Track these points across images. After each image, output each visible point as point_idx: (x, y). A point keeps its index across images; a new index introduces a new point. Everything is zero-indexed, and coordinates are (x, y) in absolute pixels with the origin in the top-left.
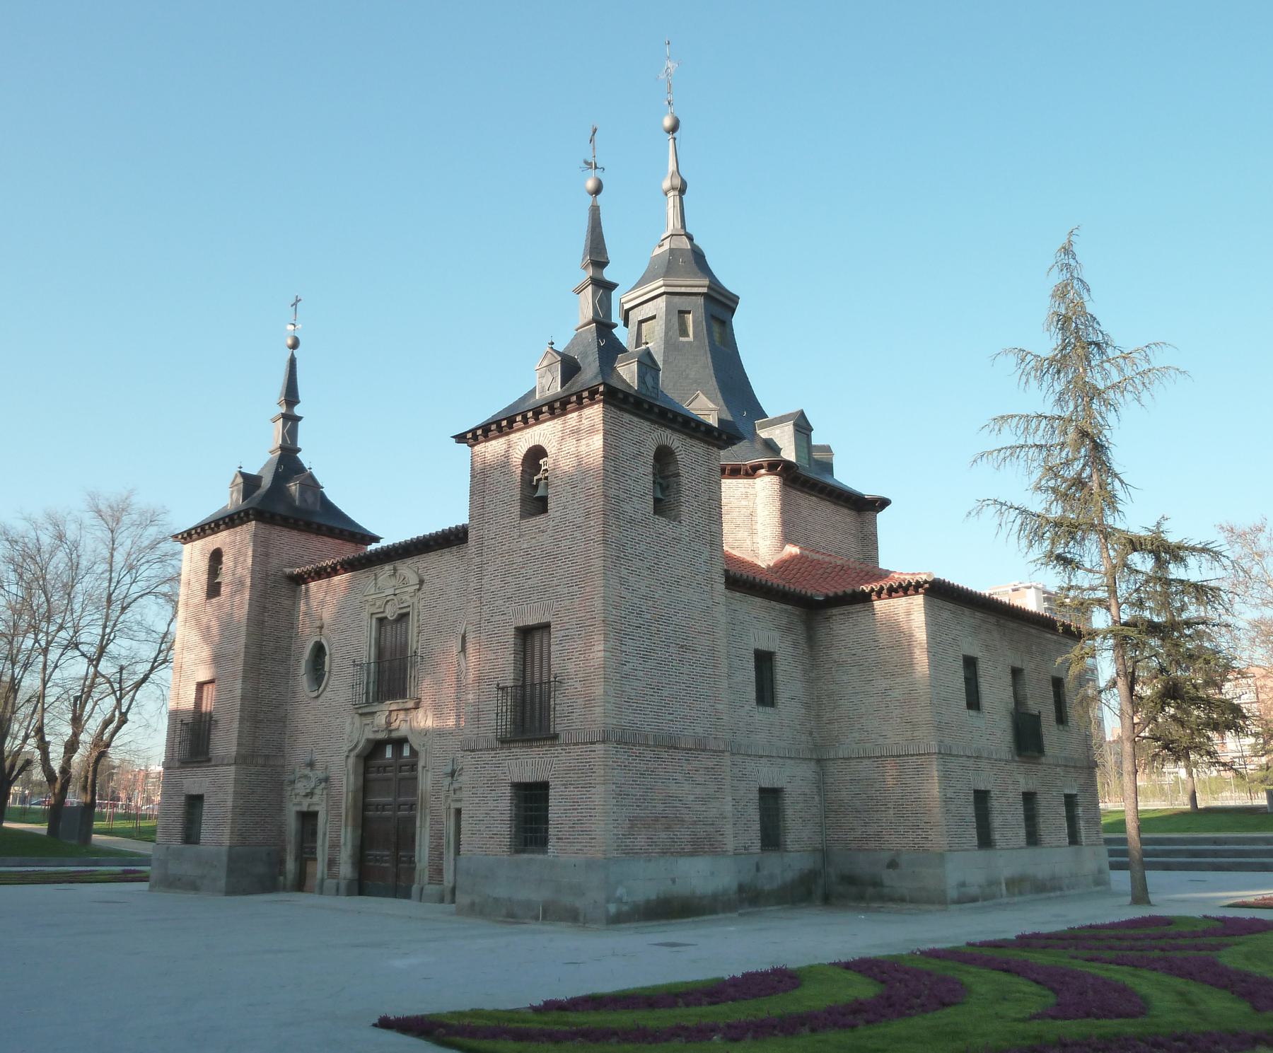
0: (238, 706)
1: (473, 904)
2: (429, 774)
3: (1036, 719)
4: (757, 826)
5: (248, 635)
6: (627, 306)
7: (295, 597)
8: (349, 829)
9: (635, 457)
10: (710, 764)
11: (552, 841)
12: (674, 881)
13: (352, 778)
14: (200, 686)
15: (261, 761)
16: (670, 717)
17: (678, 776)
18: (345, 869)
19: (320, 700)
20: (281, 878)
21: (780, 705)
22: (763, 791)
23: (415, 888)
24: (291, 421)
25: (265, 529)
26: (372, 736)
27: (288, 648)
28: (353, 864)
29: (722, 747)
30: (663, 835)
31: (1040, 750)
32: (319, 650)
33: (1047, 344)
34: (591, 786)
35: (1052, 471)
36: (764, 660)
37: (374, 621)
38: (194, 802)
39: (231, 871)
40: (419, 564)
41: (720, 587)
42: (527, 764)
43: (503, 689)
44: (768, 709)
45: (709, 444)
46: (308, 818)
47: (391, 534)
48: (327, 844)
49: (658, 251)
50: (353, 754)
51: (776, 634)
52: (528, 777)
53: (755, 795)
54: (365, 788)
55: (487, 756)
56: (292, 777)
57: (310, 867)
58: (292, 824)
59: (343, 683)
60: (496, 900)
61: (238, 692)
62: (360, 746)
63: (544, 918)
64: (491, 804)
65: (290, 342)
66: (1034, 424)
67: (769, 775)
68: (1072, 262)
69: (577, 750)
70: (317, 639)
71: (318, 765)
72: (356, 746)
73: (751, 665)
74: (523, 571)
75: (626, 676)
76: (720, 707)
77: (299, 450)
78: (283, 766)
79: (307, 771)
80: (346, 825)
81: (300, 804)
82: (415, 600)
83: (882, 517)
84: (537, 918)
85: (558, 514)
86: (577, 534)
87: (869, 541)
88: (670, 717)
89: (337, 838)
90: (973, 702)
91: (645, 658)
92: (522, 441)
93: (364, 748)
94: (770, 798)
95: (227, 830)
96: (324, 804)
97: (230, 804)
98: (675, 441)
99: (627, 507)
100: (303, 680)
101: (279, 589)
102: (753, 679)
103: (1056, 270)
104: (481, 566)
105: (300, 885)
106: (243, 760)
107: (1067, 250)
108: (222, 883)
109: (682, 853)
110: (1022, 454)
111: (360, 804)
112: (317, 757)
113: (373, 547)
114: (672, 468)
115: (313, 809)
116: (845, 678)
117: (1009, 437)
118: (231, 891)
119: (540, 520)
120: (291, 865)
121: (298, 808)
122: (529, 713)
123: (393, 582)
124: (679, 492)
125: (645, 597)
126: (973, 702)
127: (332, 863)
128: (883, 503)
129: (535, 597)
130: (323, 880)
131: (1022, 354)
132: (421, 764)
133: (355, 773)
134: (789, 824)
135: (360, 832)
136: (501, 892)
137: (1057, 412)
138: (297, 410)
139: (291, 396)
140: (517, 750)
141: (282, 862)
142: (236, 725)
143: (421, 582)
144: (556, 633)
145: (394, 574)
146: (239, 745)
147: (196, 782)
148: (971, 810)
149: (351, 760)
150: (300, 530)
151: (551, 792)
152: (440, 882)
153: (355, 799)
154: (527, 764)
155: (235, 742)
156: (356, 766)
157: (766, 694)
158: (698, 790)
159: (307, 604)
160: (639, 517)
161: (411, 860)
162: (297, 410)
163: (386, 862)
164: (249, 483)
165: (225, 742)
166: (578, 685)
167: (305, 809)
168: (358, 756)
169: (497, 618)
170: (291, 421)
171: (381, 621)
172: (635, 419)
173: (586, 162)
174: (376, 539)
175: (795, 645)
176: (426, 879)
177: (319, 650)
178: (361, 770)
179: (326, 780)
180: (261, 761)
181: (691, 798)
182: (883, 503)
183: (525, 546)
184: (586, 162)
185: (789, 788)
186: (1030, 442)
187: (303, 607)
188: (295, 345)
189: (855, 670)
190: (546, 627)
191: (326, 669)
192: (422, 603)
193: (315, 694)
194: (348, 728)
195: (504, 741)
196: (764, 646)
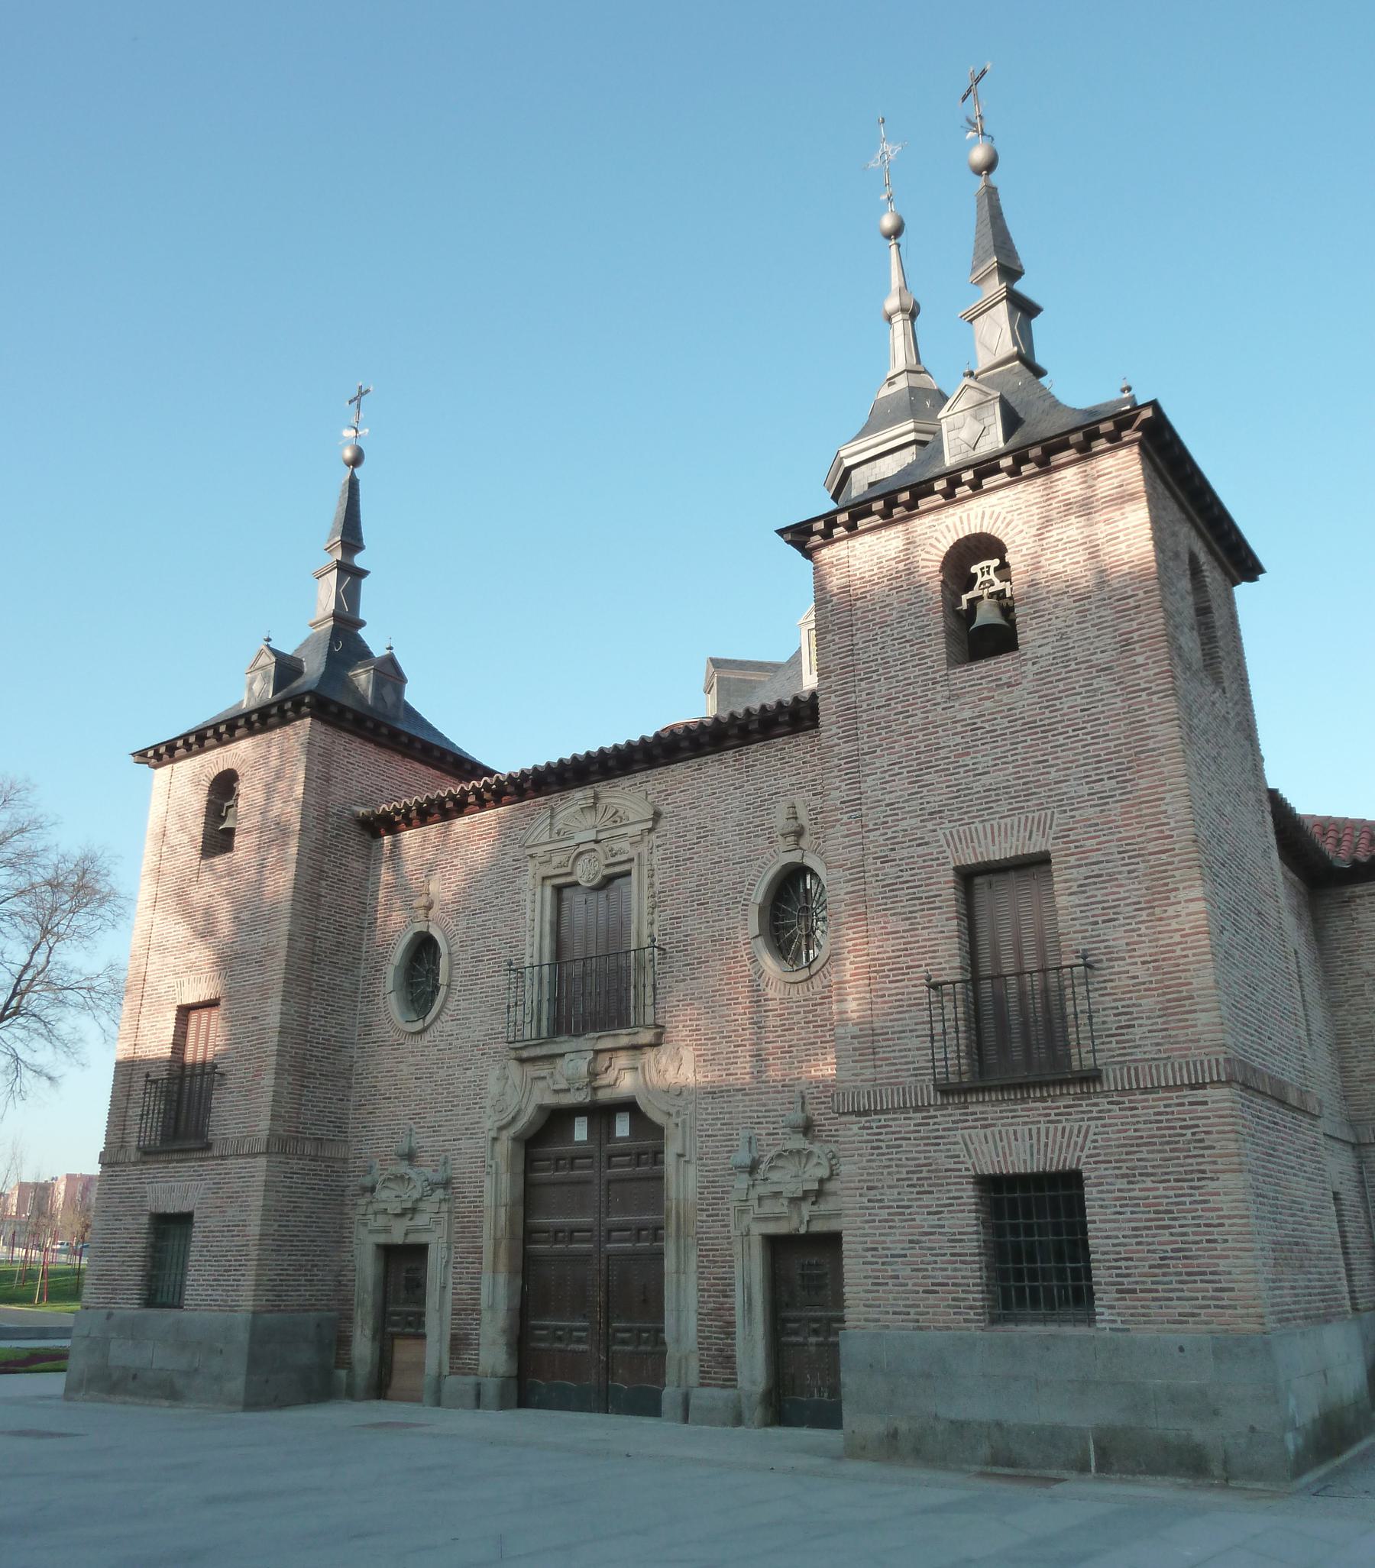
0: (273, 1046)
1: (894, 1435)
5: (295, 915)
6: (848, 463)
7: (370, 858)
8: (502, 1279)
11: (1104, 1299)
13: (505, 1178)
14: (185, 1012)
15: (309, 1149)
18: (493, 1355)
19: (427, 1037)
20: (342, 1373)
23: (670, 1394)
24: (350, 575)
25: (326, 735)
26: (550, 1100)
27: (357, 948)
28: (508, 1345)
32: (424, 948)
37: (548, 891)
38: (170, 1228)
39: (254, 1362)
40: (648, 786)
42: (1018, 1137)
43: (935, 986)
46: (404, 1261)
48: (448, 1308)
49: (886, 391)
50: (506, 1135)
52: (1021, 1160)
54: (529, 1197)
55: (903, 1124)
56: (367, 1181)
57: (403, 1352)
58: (366, 1268)
59: (479, 1007)
60: (959, 1427)
61: (274, 1020)
63: (1104, 1466)
65: (348, 454)
69: (1150, 1106)
70: (420, 927)
71: (424, 1158)
72: (514, 1119)
74: (968, 760)
77: (362, 624)
78: (345, 1160)
79: (403, 1168)
81: (387, 1230)
82: (643, 849)
84: (1084, 1468)
89: (473, 1289)
92: (942, 528)
93: (531, 1123)
95: (248, 1281)
96: (441, 1231)
97: (254, 1230)
100: (391, 1004)
101: (349, 839)
104: (855, 760)
105: (381, 1387)
106: (281, 1146)
108: (236, 1385)
112: (422, 1141)
115: (413, 1239)
118: (254, 1402)
120: (362, 1347)
121: (382, 1239)
123: (590, 819)
127: (459, 1343)
129: (1003, 807)
130: (440, 1378)
133: (511, 1166)
135: (519, 1282)
136: (977, 1409)
138: (359, 560)
139: (351, 537)
140: (982, 1108)
141: (343, 1342)
142: (268, 1080)
143: (657, 816)
144: (1064, 876)
145: (594, 806)
146: (274, 1117)
147: (174, 1188)
149: (504, 1147)
150: (378, 744)
151: (1090, 1192)
152: (730, 1382)
153: (511, 1220)
154: (1018, 1137)
155: (266, 1111)
156: (513, 1156)
159: (396, 869)
162: (359, 560)
163: (579, 1340)
164: (286, 669)
165: (245, 1113)
167: (397, 1238)
168: (515, 1139)
169: (905, 853)
170: (350, 575)
173: (969, 121)
176: (693, 1378)
177: (424, 948)
178: (520, 1167)
179: (446, 1184)
180: (309, 1149)
184: (969, 121)
187: (385, 875)
188: (356, 461)
190: (1039, 863)
191: (442, 979)
192: (658, 854)
193: (419, 1026)
194: (493, 1087)
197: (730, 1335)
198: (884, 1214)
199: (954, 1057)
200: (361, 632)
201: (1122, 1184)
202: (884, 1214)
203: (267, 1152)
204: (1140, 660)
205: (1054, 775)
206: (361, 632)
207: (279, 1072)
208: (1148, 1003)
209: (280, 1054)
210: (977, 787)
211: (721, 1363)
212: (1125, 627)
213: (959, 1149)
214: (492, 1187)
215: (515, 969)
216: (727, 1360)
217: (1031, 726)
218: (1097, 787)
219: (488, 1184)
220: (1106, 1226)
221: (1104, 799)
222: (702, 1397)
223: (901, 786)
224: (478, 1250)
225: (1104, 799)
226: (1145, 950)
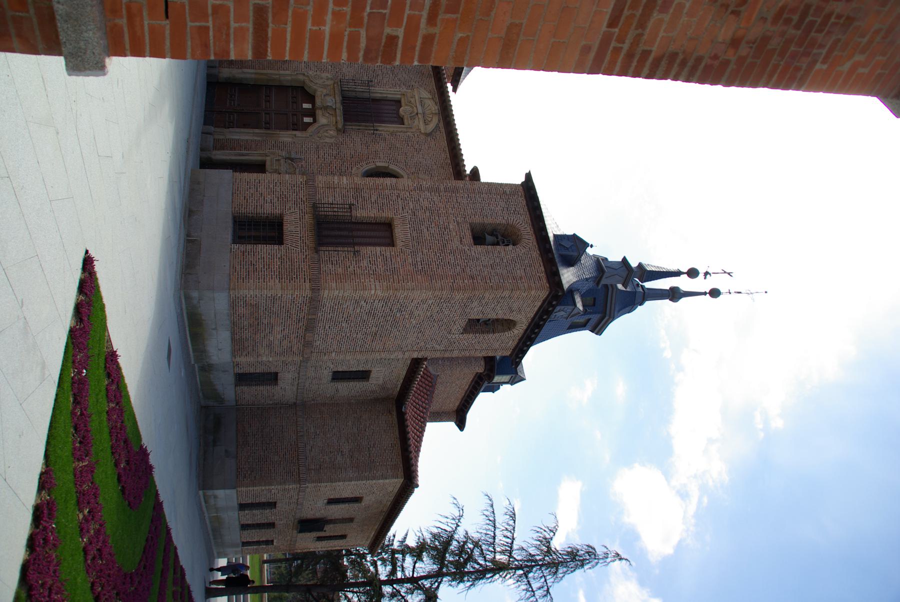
2: (290, 140)
3: (321, 529)
4: (252, 370)
8: (253, 76)
9: (510, 308)
10: (295, 349)
11: (242, 247)
12: (215, 329)
16: (327, 327)
22: (276, 374)
23: (212, 129)
26: (318, 94)
31: (301, 531)
35: (476, 544)
36: (364, 375)
37: (399, 96)
41: (415, 355)
42: (297, 226)
43: (350, 208)
44: (330, 378)
45: (514, 350)
51: (381, 382)
52: (288, 228)
53: (273, 370)
54: (282, 88)
62: (311, 84)
63: (189, 241)
64: (268, 198)
66: (509, 534)
68: (609, 560)
75: (357, 302)
76: (334, 354)
83: (451, 426)
84: (188, 235)
85: (473, 254)
87: (439, 417)
88: (327, 327)
90: (331, 502)
94: (272, 378)
98: (518, 331)
99: (475, 303)
102: (351, 370)
103: (605, 550)
104: (438, 190)
107: (618, 556)
109: (233, 334)
110: (490, 527)
111: (270, 84)
113: (450, 87)
114: (500, 327)
116: (350, 423)
117: (502, 519)
119: (469, 239)
124: (483, 332)
125: (411, 313)
126: (331, 502)
128: (461, 425)
129: (415, 234)
131: (553, 531)
132: (298, 133)
137: (515, 547)
140: (308, 219)
144: (387, 251)
148: (263, 500)
149: (301, 77)
151: (276, 247)
152: (215, 148)
154: (297, 226)
157: (338, 376)
158: (277, 342)
160: (468, 310)
161: (230, 125)
166: (352, 268)
171: (398, 103)
172: (536, 309)
174: (455, 90)
176: (217, 137)
181: (271, 339)
182: (461, 425)
183: (451, 227)
185: (278, 388)
186: (498, 532)
190: (392, 244)
194: (324, 75)
195: (315, 206)
196: (373, 375)
197: (231, 149)
198: (271, 186)
201: (279, 256)
202: (271, 186)
204: (466, 281)
208: (340, 270)
211: (221, 145)
216: (223, 148)
217: (445, 246)
218: (419, 263)
219: (288, 72)
220: (264, 250)
221: (415, 265)
222: (210, 139)
225: (415, 265)
226: (359, 271)
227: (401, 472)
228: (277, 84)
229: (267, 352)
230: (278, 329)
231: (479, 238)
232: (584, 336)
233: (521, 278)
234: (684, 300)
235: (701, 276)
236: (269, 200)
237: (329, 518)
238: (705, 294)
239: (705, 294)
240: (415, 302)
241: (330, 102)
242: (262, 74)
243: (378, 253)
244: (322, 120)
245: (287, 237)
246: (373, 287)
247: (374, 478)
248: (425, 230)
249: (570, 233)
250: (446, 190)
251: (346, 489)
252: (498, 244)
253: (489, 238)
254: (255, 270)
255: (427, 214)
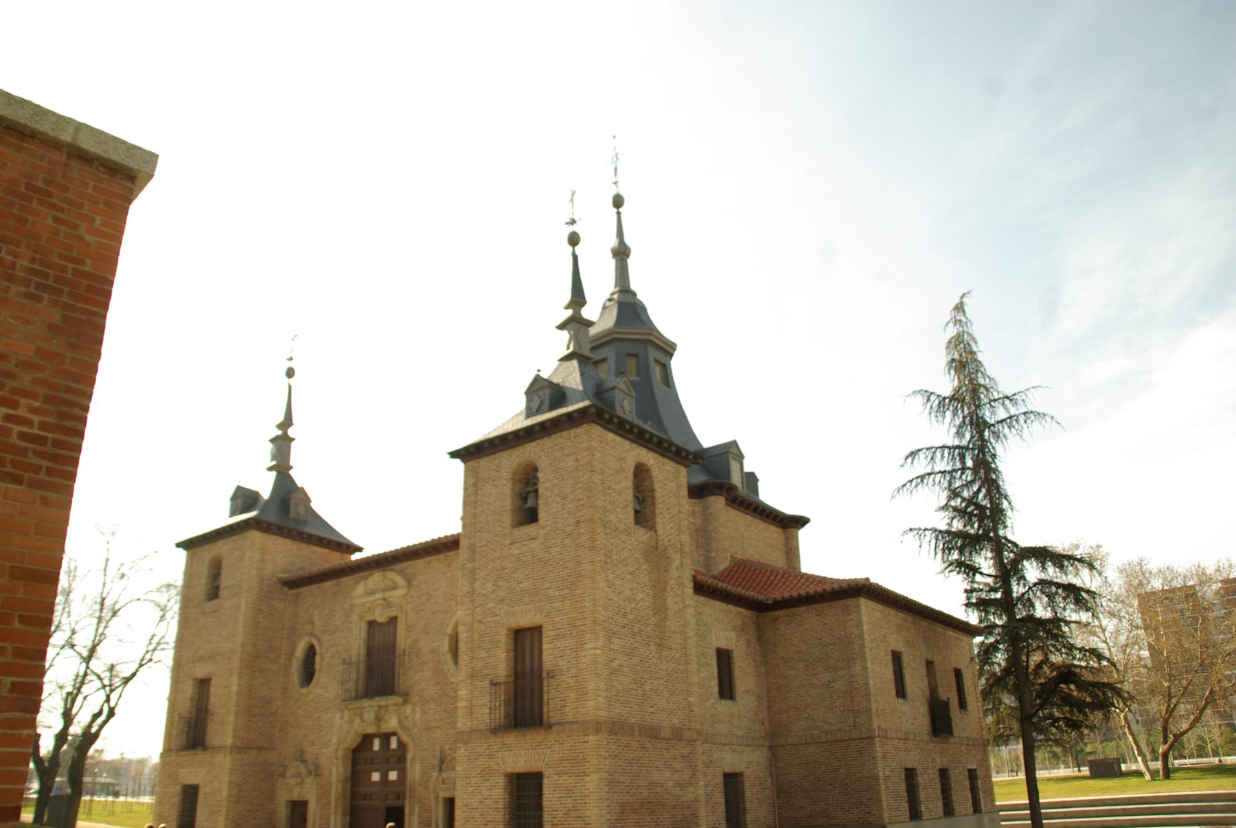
0: (233, 702)
3: (946, 704)
4: (722, 808)
8: (339, 817)
9: (618, 472)
10: (685, 752)
17: (659, 764)
21: (738, 698)
22: (726, 776)
29: (695, 737)
30: (648, 819)
33: (946, 384)
34: (585, 774)
35: (954, 494)
36: (724, 658)
41: (689, 590)
42: (521, 753)
43: (495, 684)
44: (730, 703)
45: (678, 463)
47: (372, 544)
51: (733, 634)
53: (720, 780)
58: (283, 812)
59: (330, 683)
61: (234, 688)
64: (486, 793)
67: (731, 761)
68: (964, 319)
73: (714, 662)
75: (613, 672)
76: (691, 699)
80: (336, 814)
83: (803, 534)
86: (567, 541)
87: (792, 553)
90: (901, 692)
91: (630, 656)
94: (732, 782)
97: (225, 792)
98: (650, 459)
99: (612, 517)
102: (716, 674)
103: (951, 325)
104: (473, 572)
106: (239, 749)
107: (960, 308)
111: (349, 794)
113: (355, 557)
114: (647, 483)
116: (792, 673)
119: (530, 529)
122: (524, 706)
124: (654, 505)
125: (629, 600)
126: (901, 692)
128: (801, 521)
129: (526, 599)
131: (929, 395)
132: (409, 756)
134: (748, 805)
137: (957, 443)
138: (291, 432)
140: (510, 739)
144: (547, 634)
146: (235, 737)
147: (194, 771)
148: (903, 786)
149: (341, 753)
151: (545, 781)
155: (230, 734)
157: (726, 689)
158: (676, 776)
160: (622, 527)
166: (570, 681)
167: (295, 798)
171: (372, 624)
172: (618, 438)
174: (360, 549)
175: (748, 643)
181: (671, 783)
182: (801, 521)
183: (516, 552)
185: (747, 772)
189: (801, 665)
190: (538, 629)
194: (337, 722)
195: (496, 730)
196: (723, 645)
198: (470, 789)
199: (500, 715)
200: (291, 472)
201: (556, 777)
202: (470, 789)
203: (231, 753)
205: (547, 585)
206: (291, 472)
207: (237, 714)
208: (572, 696)
209: (237, 705)
210: (518, 589)
212: (578, 514)
213: (499, 761)
214: (336, 772)
215: (347, 663)
219: (334, 770)
221: (564, 598)
223: (489, 585)
224: (329, 803)
225: (564, 598)
226: (573, 671)
227: (852, 602)
228: (349, 784)
229: (692, 789)
230: (656, 776)
231: (530, 516)
232: (679, 366)
233: (577, 460)
234: (627, 240)
235: (575, 228)
236: (488, 792)
237: (927, 693)
238: (619, 214)
239: (619, 214)
240: (611, 596)
241: (370, 716)
242: (336, 807)
243: (551, 646)
244: (392, 723)
245: (533, 767)
246: (592, 652)
247: (861, 637)
248: (521, 585)
249: (524, 397)
250: (472, 560)
251: (880, 674)
252: (536, 491)
253: (530, 503)
254: (575, 808)
255: (501, 583)
